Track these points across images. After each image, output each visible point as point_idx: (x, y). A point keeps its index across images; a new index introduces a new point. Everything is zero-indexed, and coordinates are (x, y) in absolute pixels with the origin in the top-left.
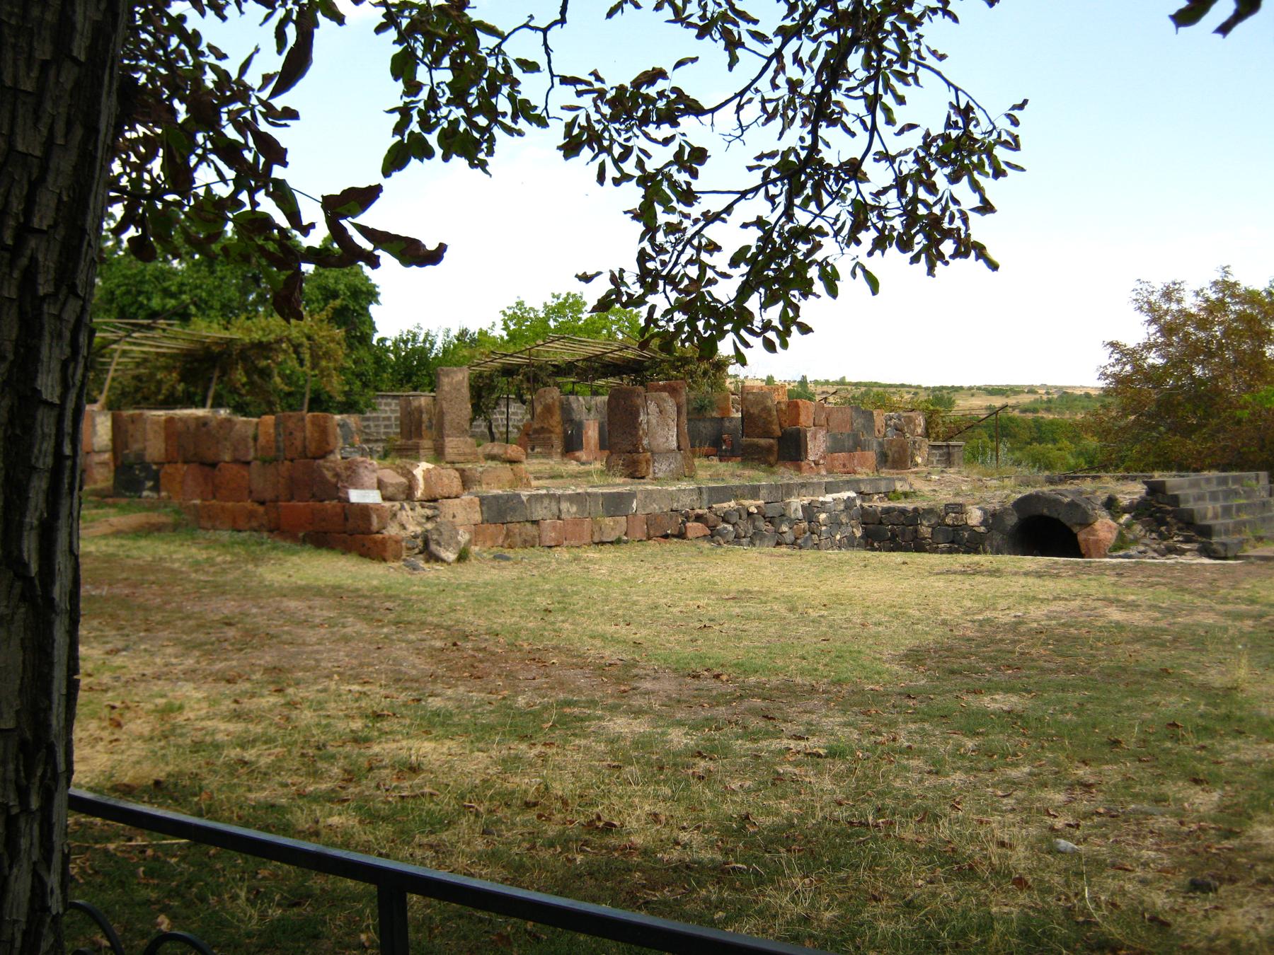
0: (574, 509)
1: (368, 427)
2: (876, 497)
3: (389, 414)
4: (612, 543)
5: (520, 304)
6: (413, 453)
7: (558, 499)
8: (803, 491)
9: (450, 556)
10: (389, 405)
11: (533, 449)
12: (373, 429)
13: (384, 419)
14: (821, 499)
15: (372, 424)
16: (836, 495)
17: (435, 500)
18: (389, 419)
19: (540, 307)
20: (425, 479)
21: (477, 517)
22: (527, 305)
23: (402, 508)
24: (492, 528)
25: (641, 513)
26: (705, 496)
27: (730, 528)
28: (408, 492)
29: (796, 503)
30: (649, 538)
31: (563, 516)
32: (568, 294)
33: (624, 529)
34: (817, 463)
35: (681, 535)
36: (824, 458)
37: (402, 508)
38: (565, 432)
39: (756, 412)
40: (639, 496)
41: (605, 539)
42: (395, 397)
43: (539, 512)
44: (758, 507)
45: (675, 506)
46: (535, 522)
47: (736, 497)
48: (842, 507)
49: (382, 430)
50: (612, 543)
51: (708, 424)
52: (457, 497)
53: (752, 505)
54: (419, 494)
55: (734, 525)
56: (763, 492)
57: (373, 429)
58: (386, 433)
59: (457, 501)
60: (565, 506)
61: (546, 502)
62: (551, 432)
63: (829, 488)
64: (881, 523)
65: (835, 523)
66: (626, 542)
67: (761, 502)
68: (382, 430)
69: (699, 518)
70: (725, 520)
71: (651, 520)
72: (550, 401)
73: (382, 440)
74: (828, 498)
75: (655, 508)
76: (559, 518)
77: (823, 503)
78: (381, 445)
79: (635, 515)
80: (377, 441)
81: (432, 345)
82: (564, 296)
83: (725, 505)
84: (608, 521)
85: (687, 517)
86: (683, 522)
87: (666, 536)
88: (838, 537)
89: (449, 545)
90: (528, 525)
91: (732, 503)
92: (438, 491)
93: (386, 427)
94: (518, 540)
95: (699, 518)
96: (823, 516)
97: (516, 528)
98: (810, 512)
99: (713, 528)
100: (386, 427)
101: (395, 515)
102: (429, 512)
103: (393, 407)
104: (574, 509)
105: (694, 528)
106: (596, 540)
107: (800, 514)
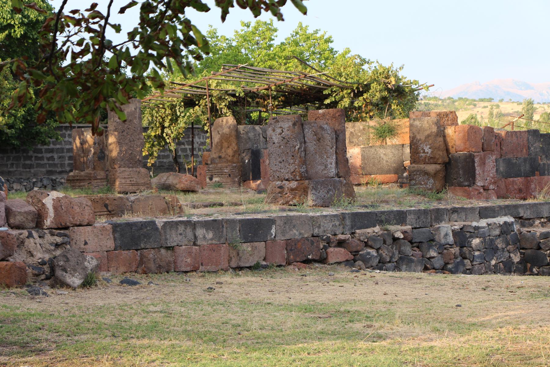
0: (210, 235)
1: (52, 158)
2: (537, 222)
4: (250, 268)
7: (193, 225)
8: (455, 216)
9: (76, 281)
11: (211, 179)
14: (474, 224)
15: (56, 156)
16: (491, 220)
17: (67, 228)
20: (55, 208)
21: (110, 244)
23: (30, 236)
24: (125, 254)
25: (280, 238)
26: (348, 222)
27: (373, 252)
28: (38, 220)
29: (446, 229)
30: (289, 263)
31: (199, 243)
33: (263, 253)
34: (486, 189)
35: (323, 260)
36: (495, 183)
37: (30, 236)
40: (278, 222)
41: (242, 264)
43: (173, 238)
44: (404, 232)
45: (316, 231)
46: (168, 248)
47: (381, 222)
48: (497, 232)
49: (67, 162)
50: (250, 268)
51: (388, 151)
52: (89, 225)
53: (398, 231)
54: (48, 222)
55: (378, 250)
56: (410, 218)
57: (57, 161)
59: (89, 228)
60: (200, 232)
61: (181, 229)
63: (484, 213)
64: (539, 248)
65: (490, 249)
66: (265, 267)
67: (408, 228)
68: (67, 162)
69: (341, 244)
70: (367, 245)
71: (290, 245)
74: (483, 223)
75: (294, 234)
76: (195, 244)
77: (477, 228)
79: (274, 240)
80: (61, 173)
83: (369, 230)
84: (247, 247)
85: (329, 242)
86: (325, 248)
87: (307, 262)
88: (493, 262)
89: (75, 270)
90: (163, 251)
91: (377, 229)
92: (68, 220)
94: (152, 266)
95: (341, 244)
96: (476, 241)
97: (151, 254)
98: (462, 237)
99: (355, 253)
101: (23, 242)
102: (59, 240)
104: (210, 235)
105: (336, 254)
106: (234, 264)
107: (451, 239)
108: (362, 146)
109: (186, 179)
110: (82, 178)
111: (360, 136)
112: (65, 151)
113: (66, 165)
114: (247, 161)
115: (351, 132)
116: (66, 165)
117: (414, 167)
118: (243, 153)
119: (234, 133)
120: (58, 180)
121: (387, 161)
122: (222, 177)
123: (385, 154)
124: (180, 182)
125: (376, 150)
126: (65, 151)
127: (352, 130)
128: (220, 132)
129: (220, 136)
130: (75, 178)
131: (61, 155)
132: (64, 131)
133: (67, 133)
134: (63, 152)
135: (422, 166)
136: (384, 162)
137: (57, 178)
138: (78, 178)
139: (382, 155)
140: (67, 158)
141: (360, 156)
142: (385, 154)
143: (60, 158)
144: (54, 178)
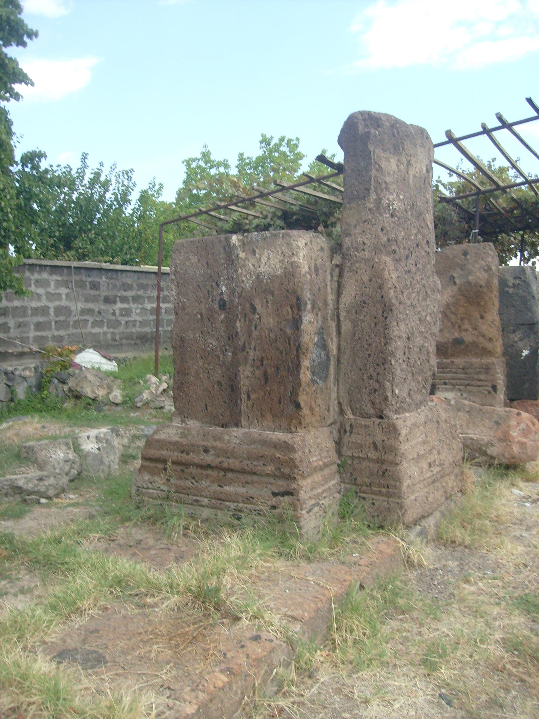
3: (44, 302)
5: (206, 156)
6: (262, 493)
10: (44, 284)
12: (14, 332)
13: (36, 311)
15: (12, 323)
18: (44, 311)
19: (233, 162)
22: (215, 157)
32: (282, 139)
38: (511, 354)
42: (55, 269)
49: (32, 334)
58: (38, 339)
68: (32, 334)
72: (478, 276)
73: (31, 354)
78: (32, 363)
80: (21, 355)
81: (106, 185)
82: (275, 141)
93: (39, 326)
100: (39, 326)
103: (52, 289)
109: (523, 426)
110: (233, 463)
112: (30, 312)
113: (31, 340)
114: (525, 353)
116: (31, 340)
118: (514, 332)
119: (496, 282)
120: (17, 373)
122: (470, 392)
124: (506, 438)
126: (30, 312)
128: (457, 281)
129: (455, 288)
130: (193, 457)
131: (21, 320)
132: (27, 274)
133: (32, 278)
134: (25, 315)
137: (16, 369)
138: (209, 459)
140: (32, 327)
143: (20, 326)
144: (10, 369)
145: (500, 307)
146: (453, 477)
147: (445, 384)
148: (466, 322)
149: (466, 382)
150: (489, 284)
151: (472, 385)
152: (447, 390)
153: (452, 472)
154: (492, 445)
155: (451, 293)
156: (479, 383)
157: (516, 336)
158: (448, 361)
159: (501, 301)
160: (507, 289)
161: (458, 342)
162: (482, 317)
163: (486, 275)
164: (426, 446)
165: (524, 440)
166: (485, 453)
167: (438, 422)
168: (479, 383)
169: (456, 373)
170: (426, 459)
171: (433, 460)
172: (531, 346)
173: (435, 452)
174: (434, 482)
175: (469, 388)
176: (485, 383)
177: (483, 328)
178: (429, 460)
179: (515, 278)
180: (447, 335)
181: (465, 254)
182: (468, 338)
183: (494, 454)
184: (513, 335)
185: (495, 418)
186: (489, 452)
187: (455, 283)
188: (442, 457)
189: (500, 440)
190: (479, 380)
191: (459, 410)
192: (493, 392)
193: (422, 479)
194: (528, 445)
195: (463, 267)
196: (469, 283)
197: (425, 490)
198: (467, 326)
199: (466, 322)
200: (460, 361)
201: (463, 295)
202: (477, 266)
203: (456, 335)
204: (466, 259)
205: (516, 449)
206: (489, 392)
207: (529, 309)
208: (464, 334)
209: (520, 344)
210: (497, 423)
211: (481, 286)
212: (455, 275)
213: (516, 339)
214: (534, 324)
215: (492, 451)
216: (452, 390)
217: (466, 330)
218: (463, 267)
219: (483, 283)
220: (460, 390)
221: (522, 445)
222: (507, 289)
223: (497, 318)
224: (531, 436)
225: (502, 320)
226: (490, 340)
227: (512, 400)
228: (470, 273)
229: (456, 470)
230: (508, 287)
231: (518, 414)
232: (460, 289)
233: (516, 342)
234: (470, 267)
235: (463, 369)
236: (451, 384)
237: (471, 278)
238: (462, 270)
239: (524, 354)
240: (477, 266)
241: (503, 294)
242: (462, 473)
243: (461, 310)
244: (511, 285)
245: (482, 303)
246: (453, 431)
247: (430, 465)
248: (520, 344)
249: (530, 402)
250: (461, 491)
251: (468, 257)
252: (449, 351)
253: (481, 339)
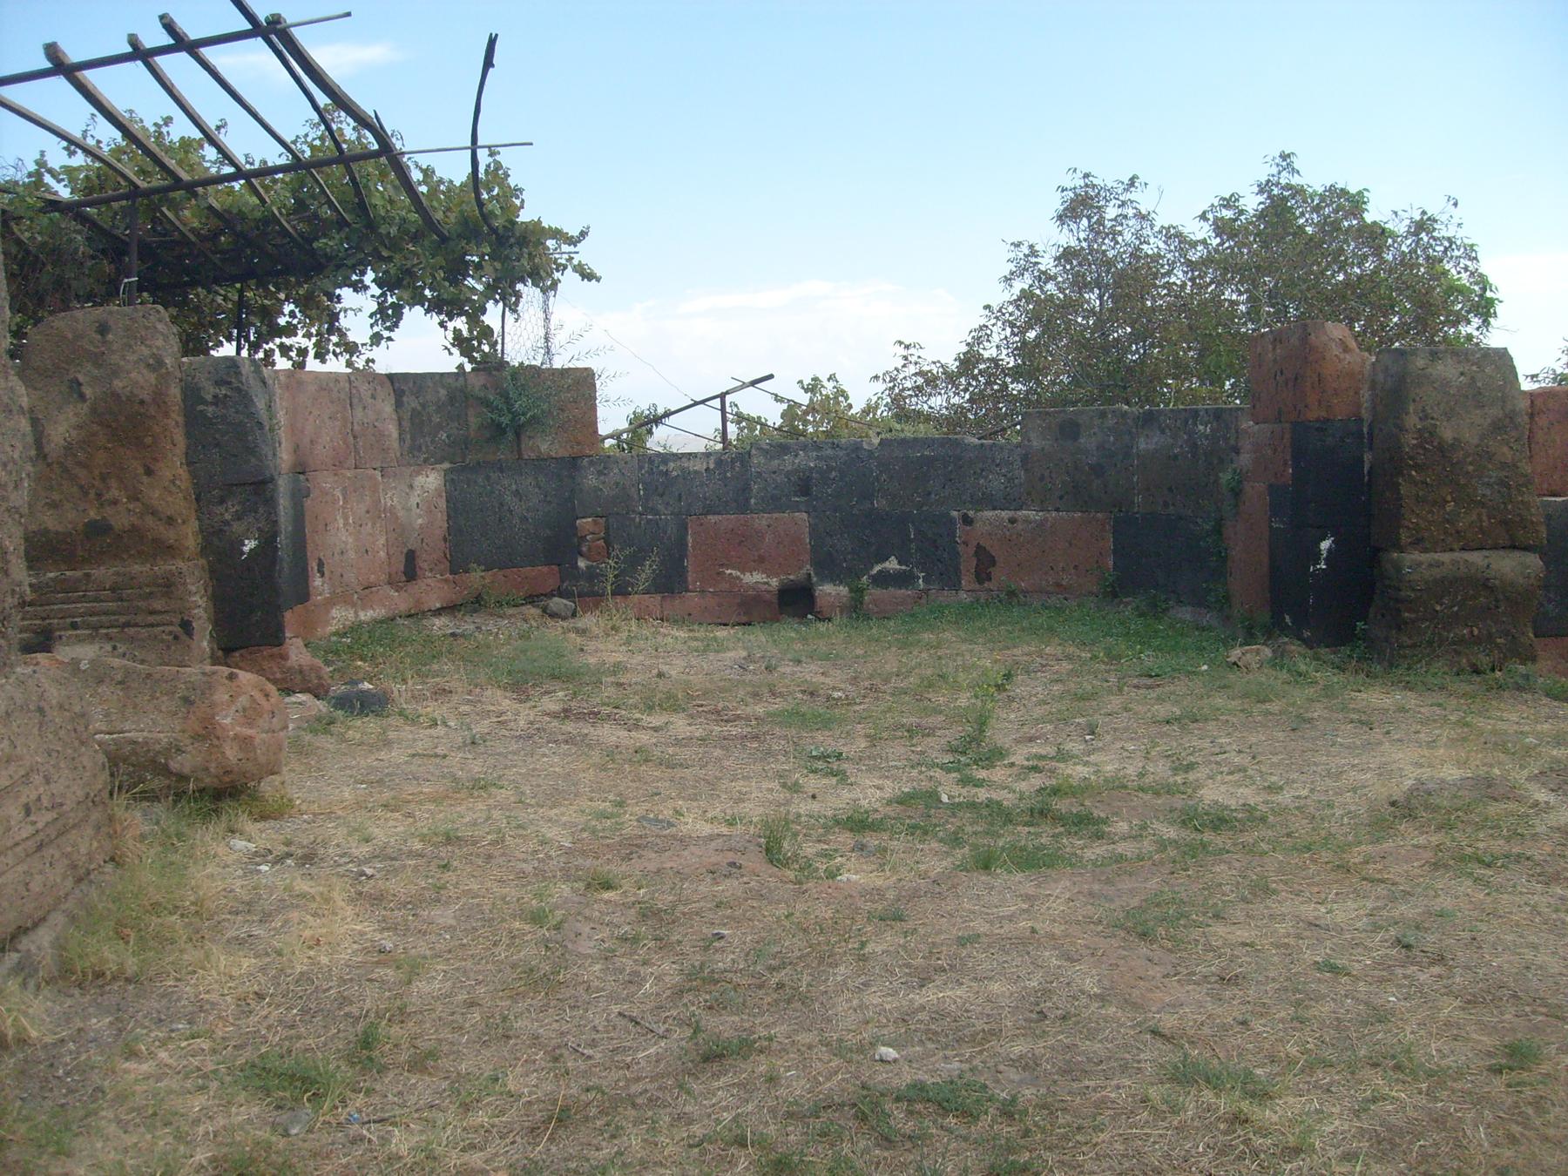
39: (1471, 437)
62: (170, 550)
72: (136, 379)
108: (446, 465)
109: (243, 701)
111: (440, 427)
114: (249, 545)
115: (414, 410)
117: (1439, 564)
118: (222, 501)
119: (175, 392)
121: (524, 519)
122: (132, 639)
123: (517, 493)
124: (208, 733)
125: (488, 478)
127: (414, 404)
128: (88, 391)
129: (84, 408)
135: (1476, 557)
136: (516, 521)
139: (508, 498)
141: (443, 504)
142: (517, 493)
145: (188, 448)
146: (90, 831)
147: (74, 626)
148: (113, 483)
149: (123, 619)
150: (159, 397)
151: (136, 625)
152: (80, 640)
153: (85, 819)
154: (179, 750)
155: (74, 420)
156: (151, 619)
157: (228, 512)
158: (79, 574)
159: (188, 435)
160: (201, 407)
161: (98, 529)
162: (149, 472)
163: (152, 378)
164: (12, 768)
165: (250, 732)
166: (165, 771)
167: (41, 710)
168: (151, 619)
169: (97, 600)
170: (17, 797)
171: (33, 796)
172: (259, 529)
173: (37, 779)
174: (40, 847)
175: (131, 631)
176: (167, 617)
177: (154, 495)
178: (24, 800)
179: (218, 383)
180: (71, 515)
181: (103, 329)
182: (120, 519)
183: (186, 771)
184: (220, 509)
185: (182, 690)
186: (174, 765)
187: (82, 397)
188: (57, 788)
189: (197, 737)
190: (152, 613)
191: (101, 681)
192: (184, 637)
193: (9, 844)
194: (257, 741)
195: (97, 359)
196: (116, 396)
197: (20, 868)
198: (115, 493)
199: (113, 483)
200: (104, 573)
201: (100, 424)
202: (132, 358)
203: (93, 514)
204: (104, 342)
205: (231, 753)
206: (176, 638)
207: (252, 450)
208: (109, 511)
209: (237, 527)
210: (187, 701)
211: (142, 402)
212: (81, 378)
213: (228, 517)
214: (264, 482)
215: (178, 763)
216: (91, 639)
217: (115, 502)
218: (97, 359)
219: (145, 395)
220: (109, 638)
221: (245, 743)
222: (201, 407)
223: (183, 472)
224: (263, 723)
225: (194, 475)
226: (170, 521)
227: (228, 651)
228: (115, 373)
229: (95, 816)
230: (205, 403)
231: (231, 677)
232: (93, 410)
233: (227, 523)
234: (115, 358)
235: (113, 590)
236: (88, 626)
237: (118, 384)
238: (98, 366)
239: (246, 549)
240: (132, 358)
241: (193, 420)
242: (111, 819)
243: (101, 457)
244: (209, 398)
245: (148, 440)
246: (81, 728)
247: (28, 812)
248: (237, 527)
249: (267, 651)
250: (112, 859)
251: (110, 337)
252: (80, 553)
253: (150, 521)
